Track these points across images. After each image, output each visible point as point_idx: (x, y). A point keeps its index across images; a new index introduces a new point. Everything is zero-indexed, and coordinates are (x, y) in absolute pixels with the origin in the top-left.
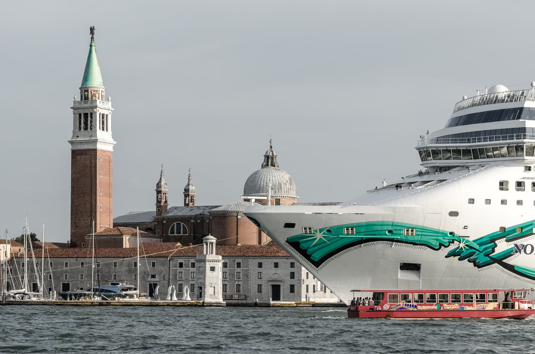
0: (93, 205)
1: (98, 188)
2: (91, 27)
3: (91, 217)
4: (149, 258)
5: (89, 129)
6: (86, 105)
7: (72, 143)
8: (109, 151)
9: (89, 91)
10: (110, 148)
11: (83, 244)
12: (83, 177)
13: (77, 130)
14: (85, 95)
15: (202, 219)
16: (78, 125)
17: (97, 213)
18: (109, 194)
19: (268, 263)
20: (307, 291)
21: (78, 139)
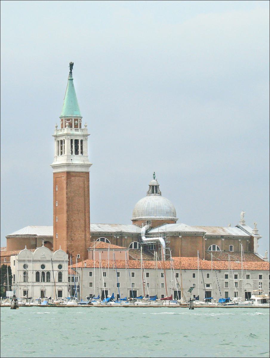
0: (87, 222)
3: (85, 232)
4: (176, 270)
5: (80, 154)
9: (79, 120)
11: (79, 255)
12: (77, 196)
14: (75, 123)
15: (121, 236)
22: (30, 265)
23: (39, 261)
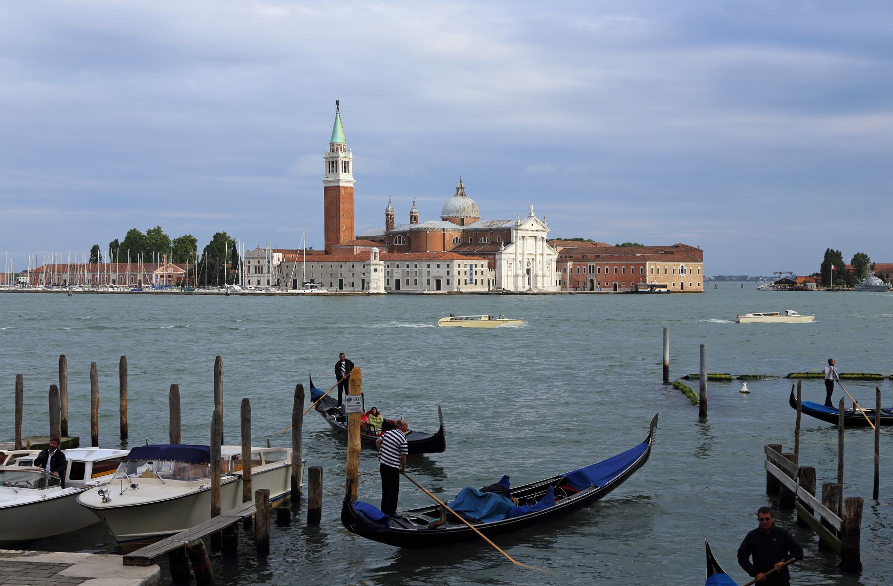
0: (338, 226)
1: (341, 213)
6: (333, 156)
7: (324, 182)
10: (352, 185)
13: (328, 173)
16: (328, 170)
19: (433, 265)
20: (459, 284)
21: (328, 179)
22: (251, 261)
23: (256, 258)
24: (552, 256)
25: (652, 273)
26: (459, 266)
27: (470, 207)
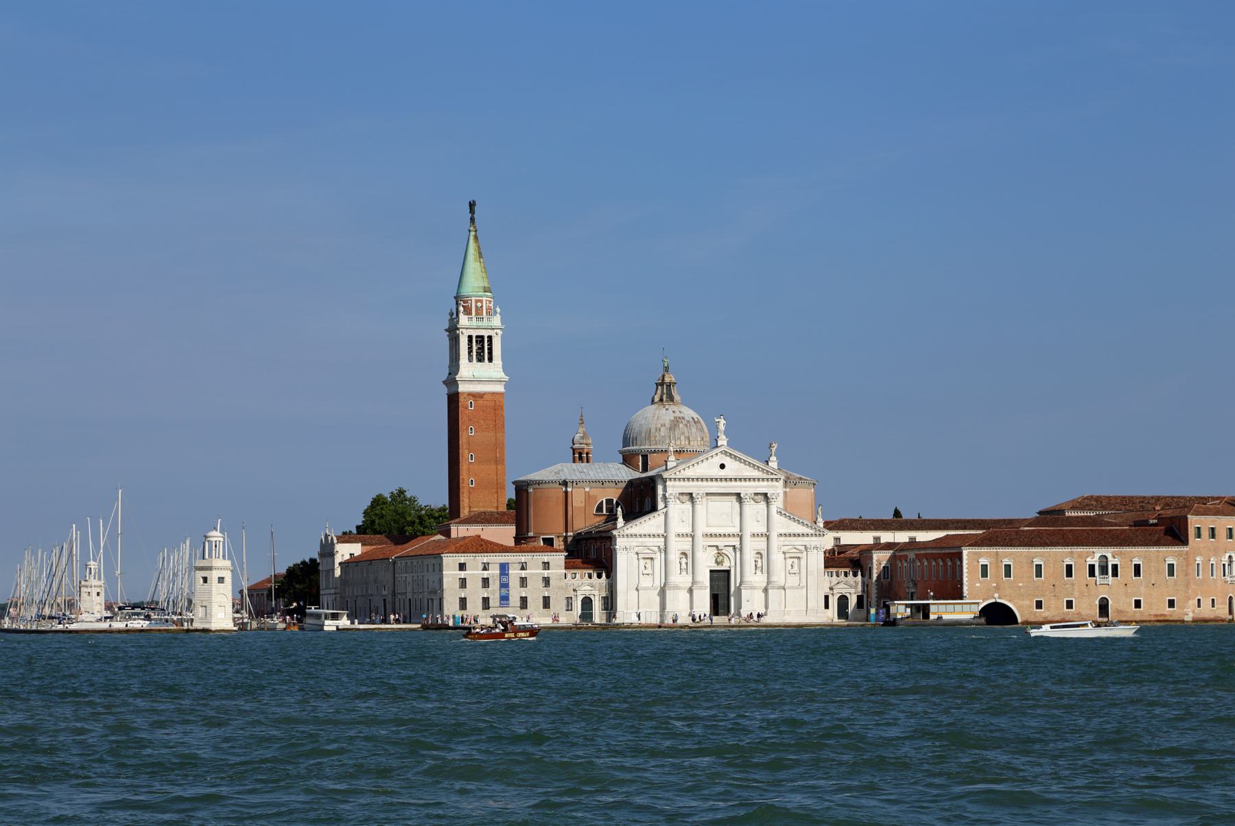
2: (470, 202)
8: (494, 393)
10: (500, 388)
17: (461, 491)
18: (495, 459)
24: (806, 539)
25: (985, 574)
26: (462, 567)
27: (663, 429)
